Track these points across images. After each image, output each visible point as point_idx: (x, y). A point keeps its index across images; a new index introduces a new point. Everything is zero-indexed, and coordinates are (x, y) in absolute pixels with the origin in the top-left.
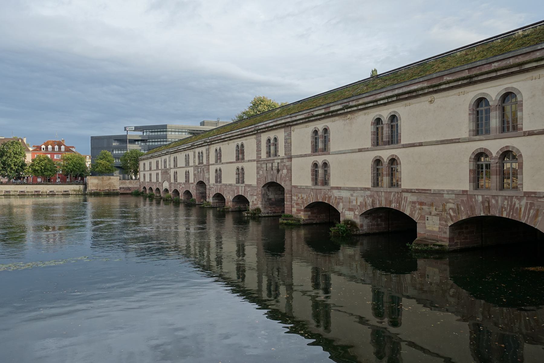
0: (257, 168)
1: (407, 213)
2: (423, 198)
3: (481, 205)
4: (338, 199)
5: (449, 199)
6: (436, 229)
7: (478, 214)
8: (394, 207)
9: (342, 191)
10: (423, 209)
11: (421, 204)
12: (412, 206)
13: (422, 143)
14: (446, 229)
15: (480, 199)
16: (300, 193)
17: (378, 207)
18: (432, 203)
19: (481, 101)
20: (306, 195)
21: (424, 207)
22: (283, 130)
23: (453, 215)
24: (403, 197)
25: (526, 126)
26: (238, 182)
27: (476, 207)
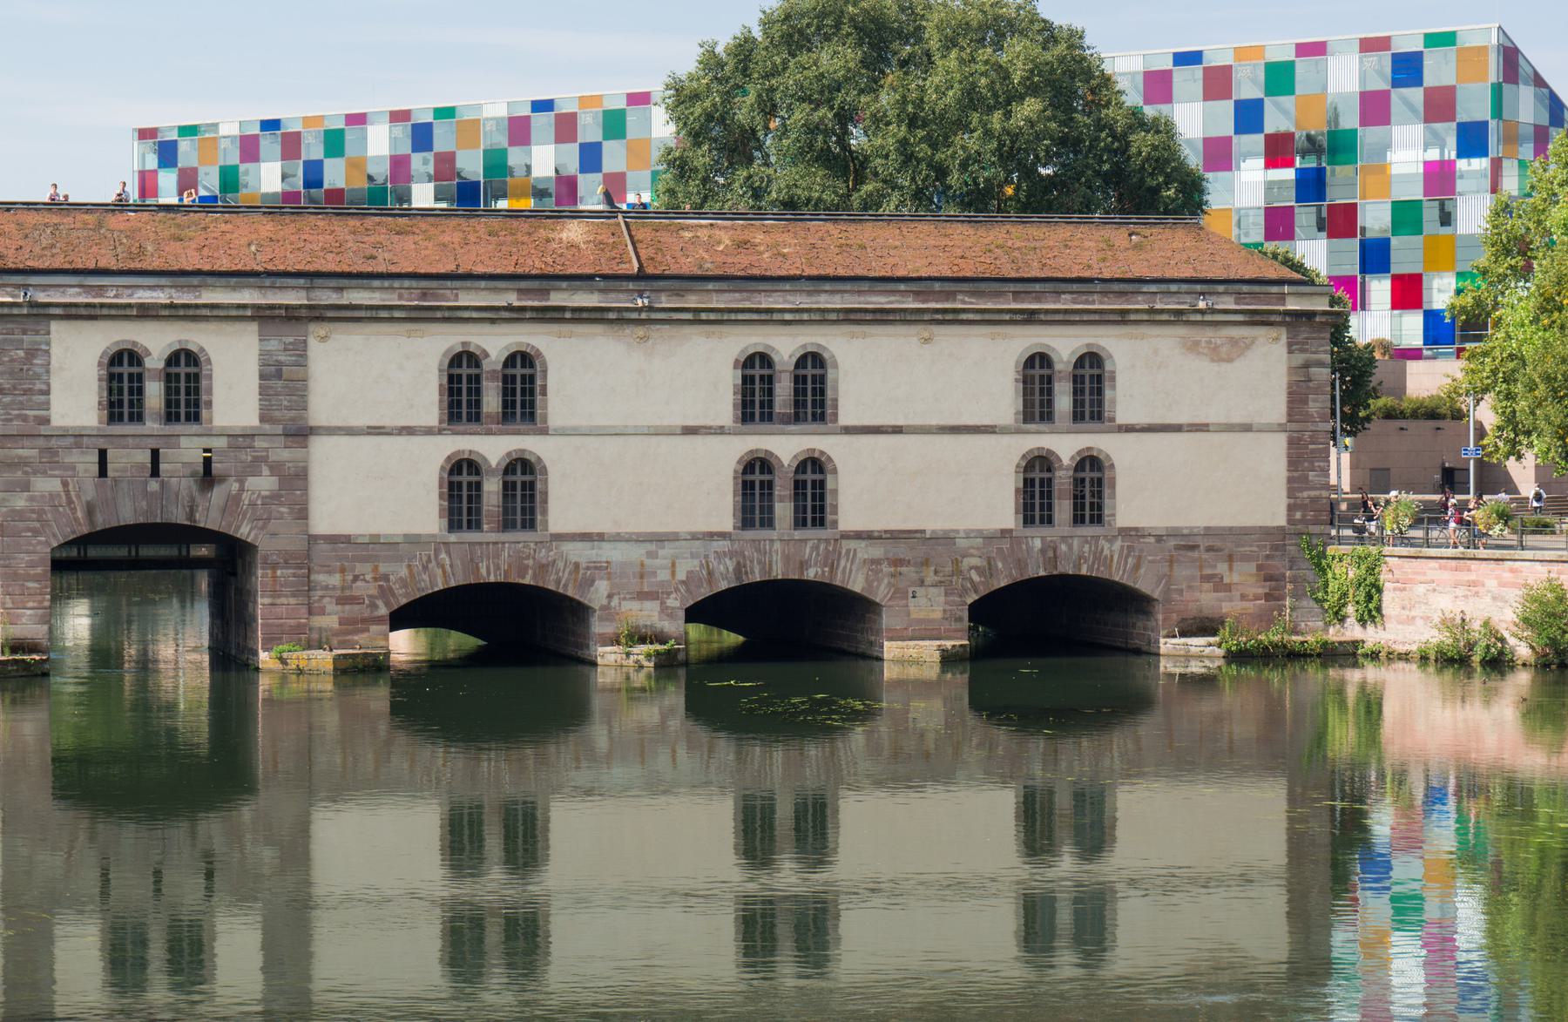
1: (857, 585)
2: (902, 550)
4: (588, 568)
5: (969, 548)
8: (815, 577)
9: (604, 544)
10: (900, 574)
11: (898, 562)
14: (962, 610)
15: (1038, 543)
16: (364, 560)
17: (758, 580)
20: (409, 566)
21: (904, 569)
22: (253, 327)
24: (844, 551)
25: (1121, 418)
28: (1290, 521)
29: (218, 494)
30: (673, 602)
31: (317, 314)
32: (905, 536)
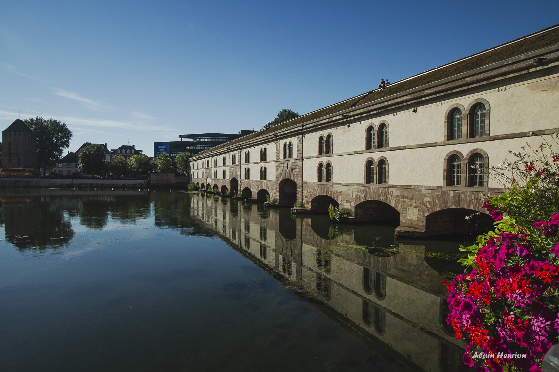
1: (393, 205)
2: (405, 193)
3: (453, 199)
5: (426, 194)
6: (415, 218)
7: (450, 207)
11: (404, 197)
12: (396, 199)
13: (406, 146)
15: (452, 193)
18: (413, 197)
19: (454, 111)
21: (406, 200)
23: (429, 207)
24: (390, 192)
26: (261, 179)
27: (448, 201)
32: (406, 187)
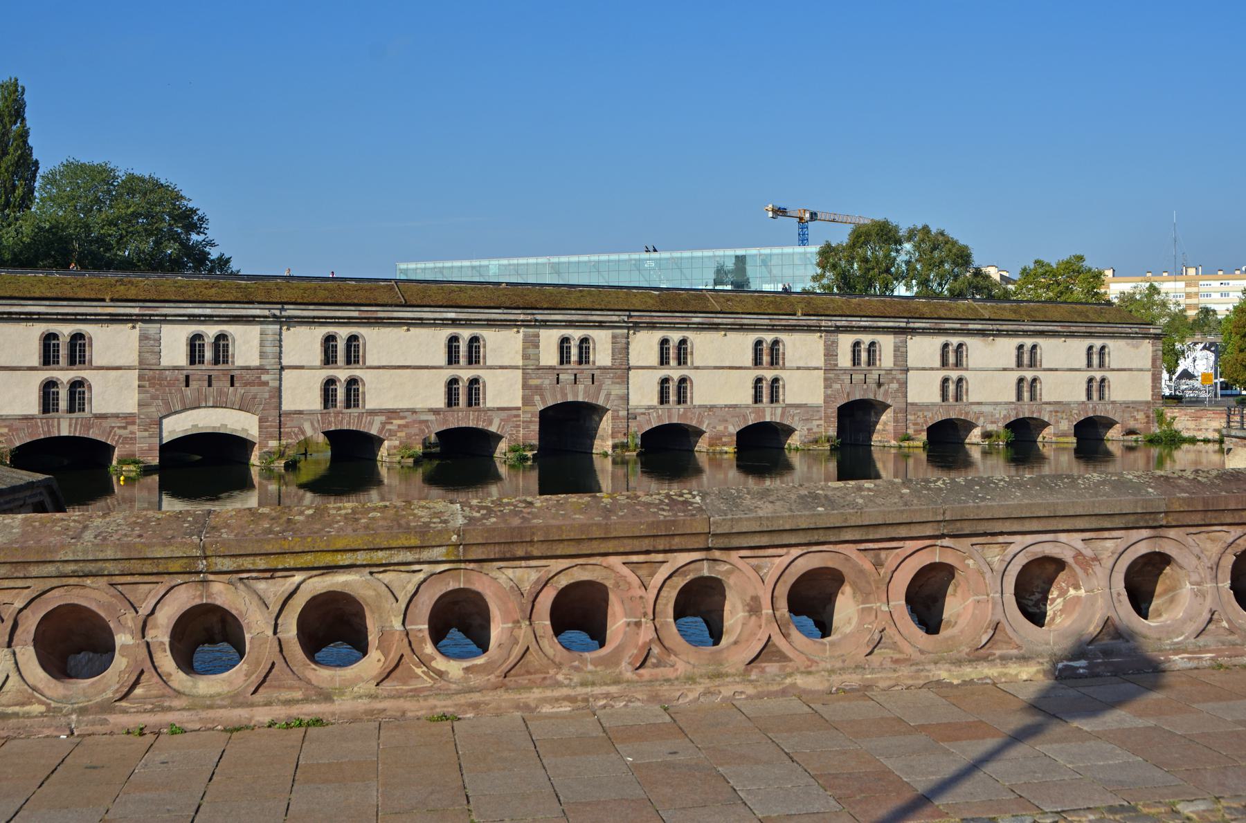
0: (826, 379)
1: (1046, 419)
2: (1057, 408)
6: (1066, 428)
11: (1056, 412)
15: (1091, 406)
28: (1153, 399)
29: (882, 389)
30: (1000, 425)
31: (914, 332)
